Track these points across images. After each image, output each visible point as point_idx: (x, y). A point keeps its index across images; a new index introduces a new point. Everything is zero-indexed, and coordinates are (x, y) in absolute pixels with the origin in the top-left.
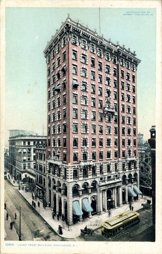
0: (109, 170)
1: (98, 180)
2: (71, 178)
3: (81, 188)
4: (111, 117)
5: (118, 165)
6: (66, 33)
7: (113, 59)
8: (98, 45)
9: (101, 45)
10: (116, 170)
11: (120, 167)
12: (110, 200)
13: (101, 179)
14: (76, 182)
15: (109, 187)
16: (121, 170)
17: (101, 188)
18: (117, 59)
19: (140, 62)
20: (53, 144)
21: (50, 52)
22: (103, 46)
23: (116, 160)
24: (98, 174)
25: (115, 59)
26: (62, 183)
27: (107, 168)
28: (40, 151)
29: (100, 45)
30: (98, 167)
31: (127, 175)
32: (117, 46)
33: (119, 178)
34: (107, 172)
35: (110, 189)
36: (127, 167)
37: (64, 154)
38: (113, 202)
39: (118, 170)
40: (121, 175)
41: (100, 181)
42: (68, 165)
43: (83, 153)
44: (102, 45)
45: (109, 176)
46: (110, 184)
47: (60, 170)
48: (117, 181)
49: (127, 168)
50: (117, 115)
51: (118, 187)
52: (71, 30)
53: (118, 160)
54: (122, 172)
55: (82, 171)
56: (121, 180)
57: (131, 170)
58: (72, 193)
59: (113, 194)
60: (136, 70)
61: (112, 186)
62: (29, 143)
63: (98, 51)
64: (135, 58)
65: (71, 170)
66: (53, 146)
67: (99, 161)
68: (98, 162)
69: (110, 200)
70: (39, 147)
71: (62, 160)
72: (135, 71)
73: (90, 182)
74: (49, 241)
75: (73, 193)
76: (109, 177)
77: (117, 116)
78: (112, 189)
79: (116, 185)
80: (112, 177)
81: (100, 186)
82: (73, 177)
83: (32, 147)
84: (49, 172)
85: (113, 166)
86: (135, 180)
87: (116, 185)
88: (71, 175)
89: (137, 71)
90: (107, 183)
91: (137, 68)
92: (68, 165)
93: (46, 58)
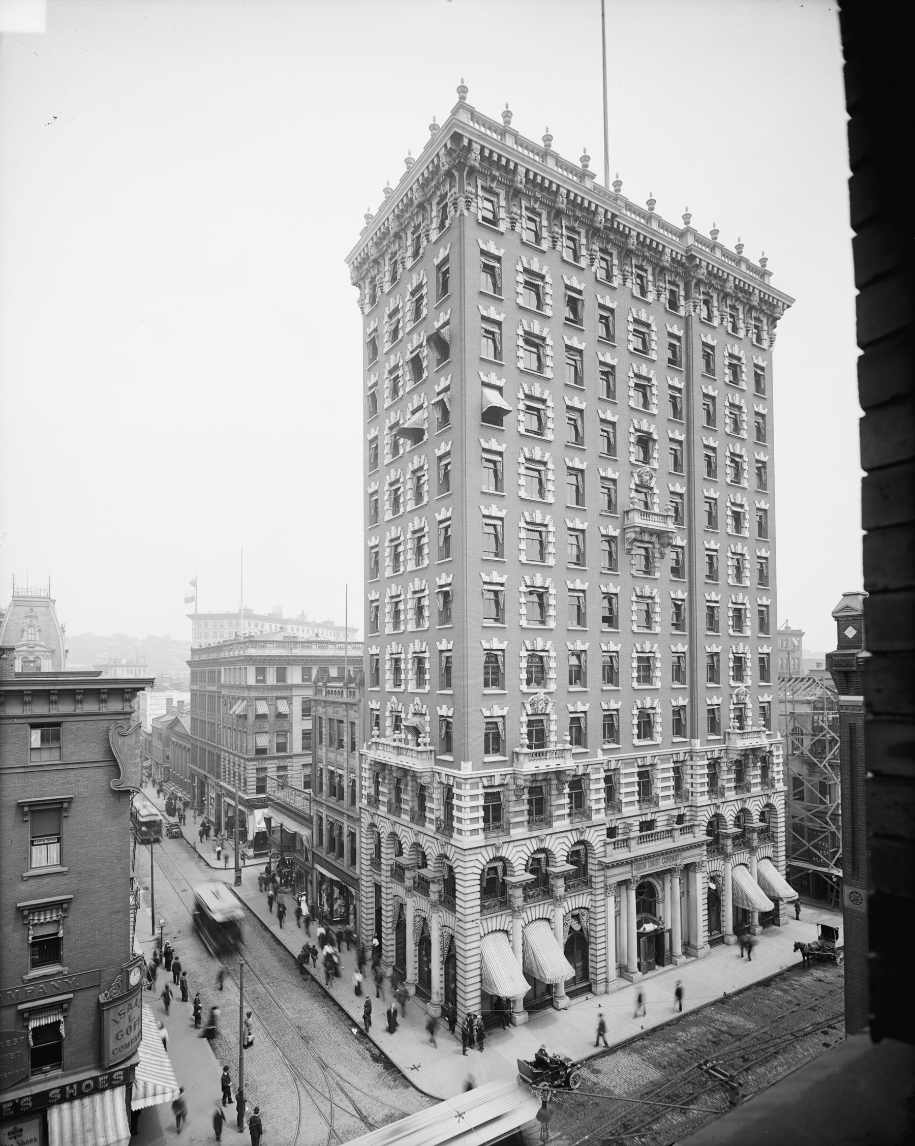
1: (596, 837)
2: (474, 832)
4: (657, 555)
5: (690, 772)
6: (449, 174)
7: (667, 292)
8: (598, 230)
9: (611, 229)
11: (698, 778)
13: (611, 832)
15: (649, 869)
16: (702, 793)
17: (610, 872)
18: (682, 293)
19: (788, 306)
21: (376, 262)
22: (622, 234)
23: (682, 749)
24: (598, 810)
25: (672, 292)
26: (432, 850)
28: (330, 710)
29: (605, 228)
31: (729, 813)
32: (682, 235)
33: (691, 826)
35: (650, 879)
36: (729, 780)
40: (704, 817)
41: (605, 844)
42: (460, 770)
44: (617, 231)
45: (649, 818)
47: (422, 793)
48: (683, 840)
49: (727, 786)
50: (683, 543)
51: (689, 868)
52: (474, 158)
53: (687, 748)
55: (526, 796)
57: (748, 790)
58: (478, 895)
59: (663, 902)
60: (772, 342)
61: (661, 866)
62: (281, 675)
63: (599, 254)
64: (769, 287)
67: (600, 752)
69: (649, 927)
70: (328, 693)
71: (432, 748)
72: (765, 345)
73: (560, 847)
76: (647, 826)
77: (682, 547)
78: (660, 875)
79: (678, 862)
80: (661, 824)
82: (481, 824)
83: (295, 692)
84: (374, 801)
86: (767, 834)
87: (678, 862)
89: (776, 344)
91: (775, 331)
92: (460, 770)
93: (360, 287)
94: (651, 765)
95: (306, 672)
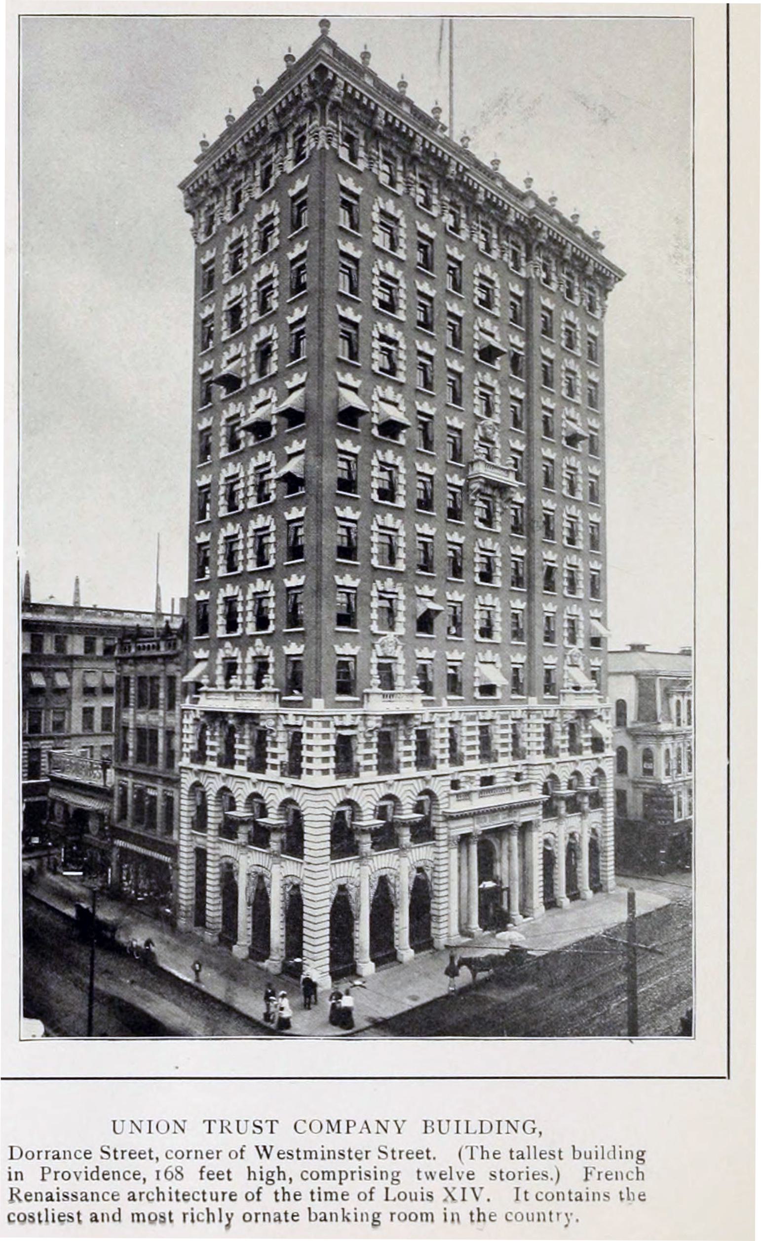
0: (487, 753)
1: (440, 788)
2: (325, 772)
3: (369, 820)
4: (499, 509)
5: (526, 730)
7: (510, 252)
8: (449, 180)
9: (460, 182)
10: (517, 753)
11: (532, 739)
12: (489, 884)
13: (455, 784)
14: (348, 790)
15: (490, 823)
16: (538, 752)
17: (453, 824)
18: (524, 255)
19: (620, 280)
20: (221, 621)
23: (519, 707)
24: (442, 761)
25: (515, 253)
26: (274, 797)
27: (480, 738)
28: (141, 668)
29: (456, 180)
30: (442, 730)
31: (564, 774)
33: (528, 785)
34: (480, 757)
35: (486, 837)
37: (287, 661)
38: (505, 893)
39: (524, 749)
40: (540, 776)
41: (450, 795)
42: (310, 707)
43: (378, 657)
44: (466, 185)
45: (488, 774)
46: (493, 811)
47: (260, 741)
48: (518, 797)
50: (522, 500)
51: (526, 828)
52: (337, 94)
53: (525, 707)
54: (541, 759)
55: (375, 740)
56: (536, 793)
58: (328, 837)
59: (500, 861)
60: (603, 313)
61: (501, 821)
62: (60, 645)
63: (449, 207)
64: (603, 259)
65: (326, 730)
66: (221, 633)
67: (445, 703)
68: (440, 705)
69: (489, 884)
70: (139, 648)
71: (277, 690)
72: (598, 315)
73: (408, 795)
74: (359, 910)
75: (332, 841)
76: (487, 781)
77: (521, 505)
78: (501, 832)
79: (516, 819)
80: (500, 782)
81: (450, 818)
82: (332, 765)
83: (76, 664)
84: (199, 756)
85: (504, 731)
86: (597, 801)
87: (516, 819)
88: (326, 754)
89: (607, 315)
90: (478, 803)
91: (607, 302)
92: (310, 707)
93: (194, 215)
94: (491, 720)
95: (89, 646)
